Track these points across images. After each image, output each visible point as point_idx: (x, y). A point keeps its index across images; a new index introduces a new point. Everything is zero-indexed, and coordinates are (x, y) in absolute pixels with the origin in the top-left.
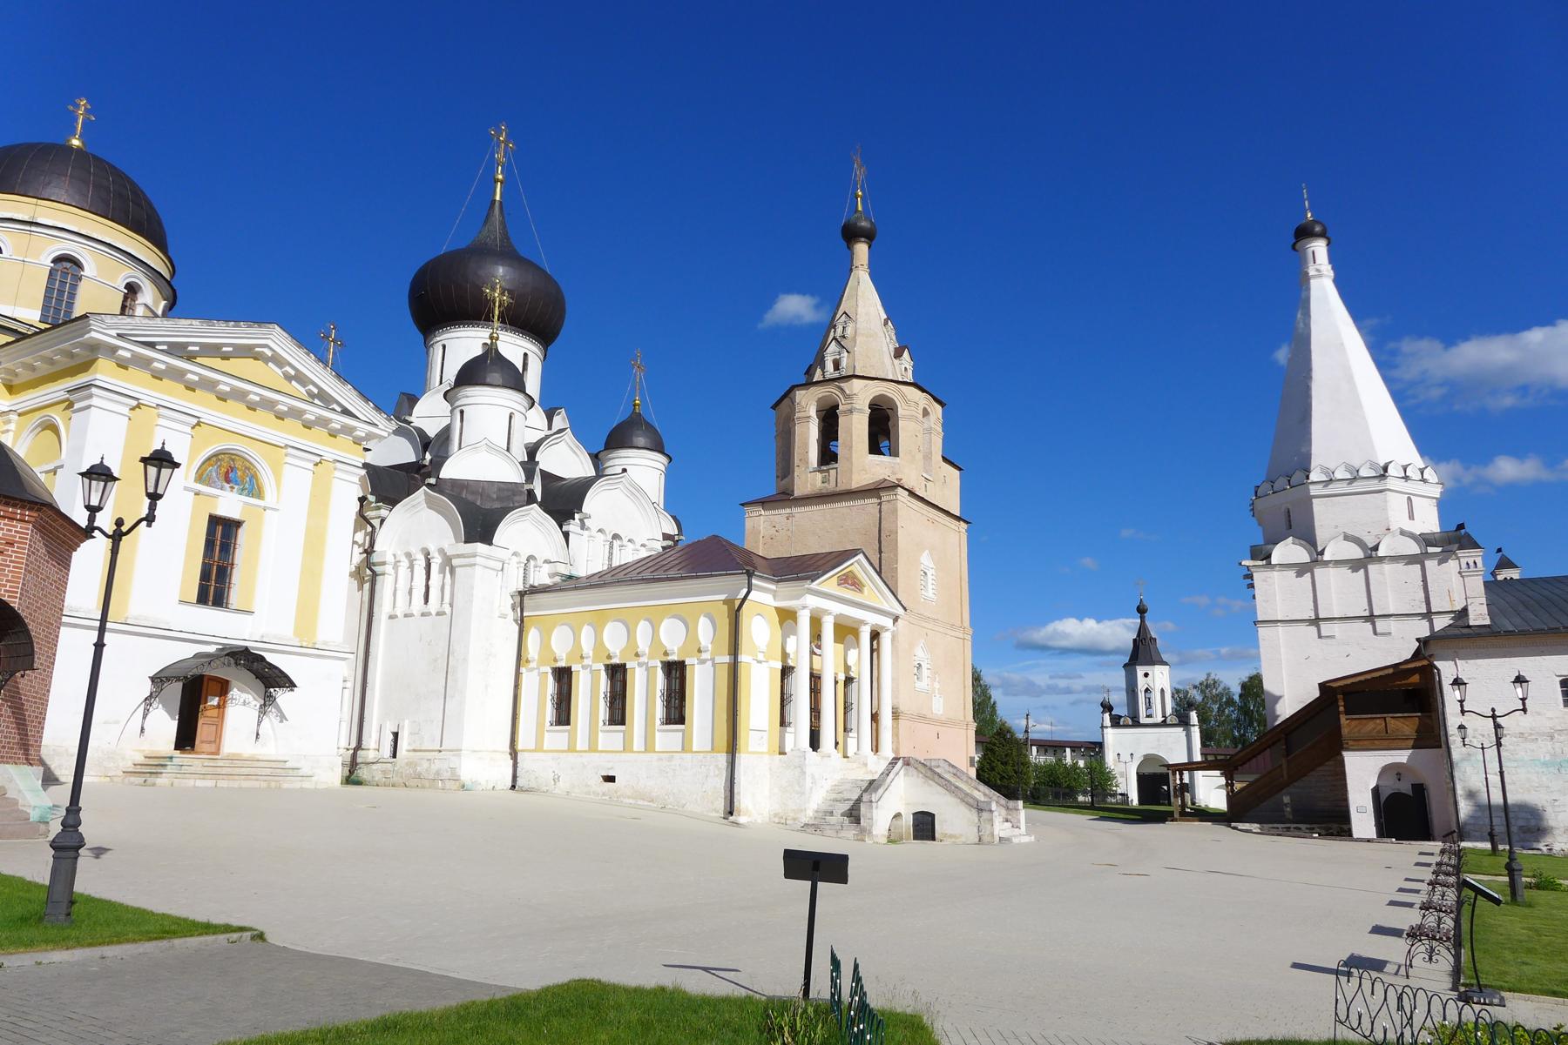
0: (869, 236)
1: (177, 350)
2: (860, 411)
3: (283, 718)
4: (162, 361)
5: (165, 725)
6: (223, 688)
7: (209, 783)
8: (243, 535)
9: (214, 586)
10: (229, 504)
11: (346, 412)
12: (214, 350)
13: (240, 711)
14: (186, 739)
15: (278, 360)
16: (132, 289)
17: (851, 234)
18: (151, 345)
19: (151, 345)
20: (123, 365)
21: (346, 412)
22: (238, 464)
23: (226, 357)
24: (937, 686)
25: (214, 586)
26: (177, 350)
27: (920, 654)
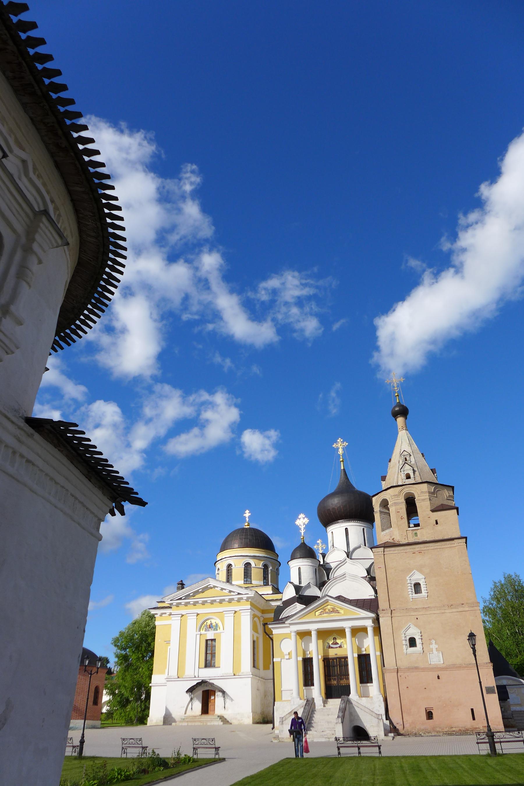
0: (403, 412)
1: (187, 597)
2: (377, 512)
3: (232, 700)
4: (183, 602)
5: (198, 705)
6: (213, 693)
7: (186, 724)
8: (217, 644)
9: (209, 662)
10: (210, 635)
11: (239, 594)
12: (197, 592)
13: (218, 700)
14: (205, 710)
15: (215, 587)
16: (247, 566)
17: (395, 415)
18: (180, 599)
19: (180, 599)
20: (178, 605)
21: (239, 594)
22: (213, 621)
23: (203, 592)
24: (434, 646)
25: (209, 662)
26: (187, 597)
27: (414, 632)
